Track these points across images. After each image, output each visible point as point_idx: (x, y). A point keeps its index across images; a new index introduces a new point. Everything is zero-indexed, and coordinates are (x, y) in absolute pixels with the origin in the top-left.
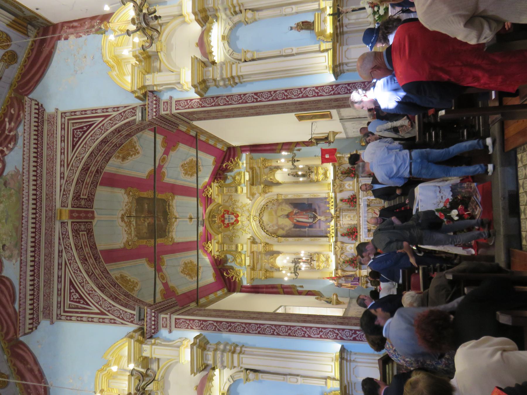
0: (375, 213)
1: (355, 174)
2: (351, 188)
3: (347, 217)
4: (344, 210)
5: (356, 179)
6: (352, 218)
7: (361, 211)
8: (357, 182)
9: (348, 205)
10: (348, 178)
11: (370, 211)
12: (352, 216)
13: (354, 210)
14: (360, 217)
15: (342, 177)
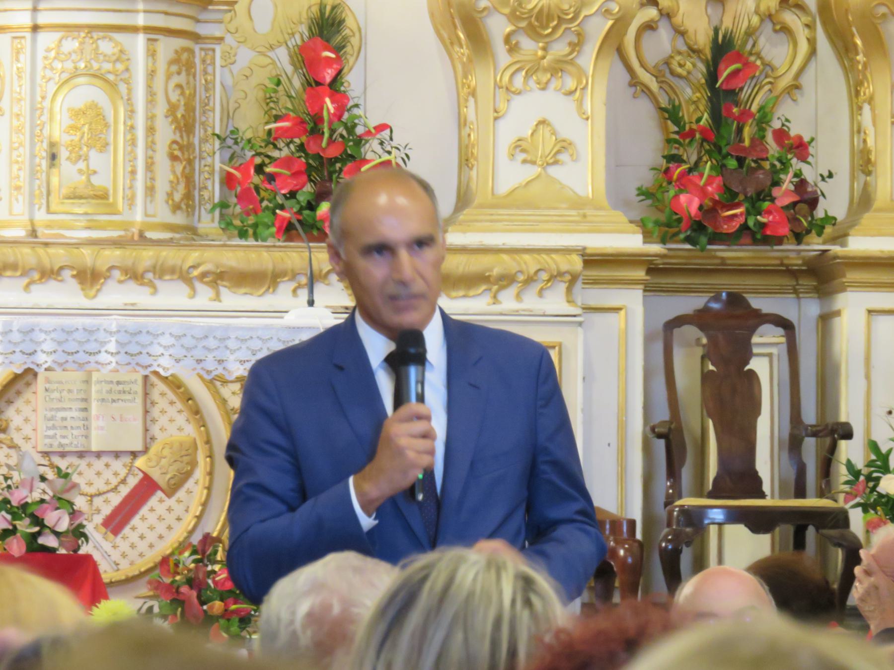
0: (147, 487)
1: (700, 229)
2: (510, 175)
3: (87, 93)
4: (183, 63)
5: (632, 242)
6: (68, 174)
7: (173, 295)
8: (593, 260)
9: (251, 122)
10: (647, 145)
11: (174, 427)
12: (106, 169)
13: (187, 202)
14: (90, 278)
15: (662, 43)
